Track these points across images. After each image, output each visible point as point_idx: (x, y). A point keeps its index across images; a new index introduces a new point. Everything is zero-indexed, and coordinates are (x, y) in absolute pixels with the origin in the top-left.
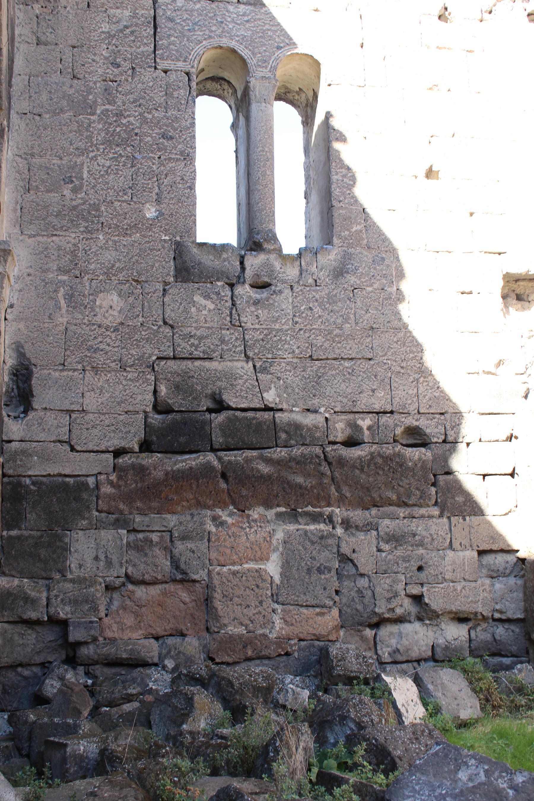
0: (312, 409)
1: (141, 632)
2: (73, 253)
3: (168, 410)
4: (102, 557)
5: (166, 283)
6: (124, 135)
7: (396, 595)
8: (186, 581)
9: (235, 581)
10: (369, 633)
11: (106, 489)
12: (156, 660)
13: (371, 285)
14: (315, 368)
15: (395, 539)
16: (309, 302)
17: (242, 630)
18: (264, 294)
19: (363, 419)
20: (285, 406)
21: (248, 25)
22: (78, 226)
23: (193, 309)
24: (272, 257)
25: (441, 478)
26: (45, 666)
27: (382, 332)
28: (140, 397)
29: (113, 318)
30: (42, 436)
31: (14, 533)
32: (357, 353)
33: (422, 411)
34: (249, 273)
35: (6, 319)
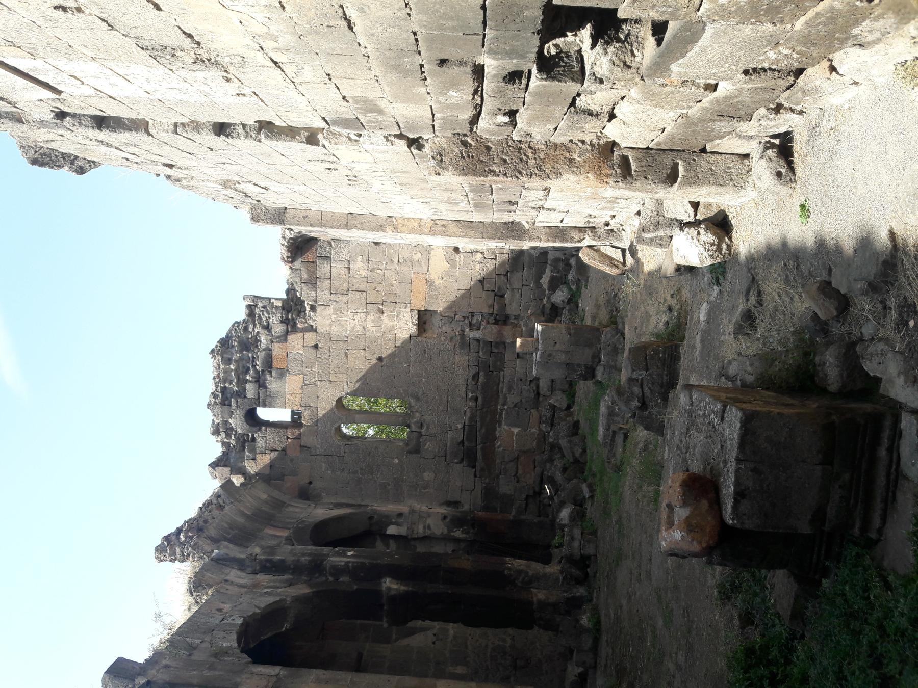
8: (518, 458)
10: (541, 399)
15: (510, 388)
17: (535, 443)
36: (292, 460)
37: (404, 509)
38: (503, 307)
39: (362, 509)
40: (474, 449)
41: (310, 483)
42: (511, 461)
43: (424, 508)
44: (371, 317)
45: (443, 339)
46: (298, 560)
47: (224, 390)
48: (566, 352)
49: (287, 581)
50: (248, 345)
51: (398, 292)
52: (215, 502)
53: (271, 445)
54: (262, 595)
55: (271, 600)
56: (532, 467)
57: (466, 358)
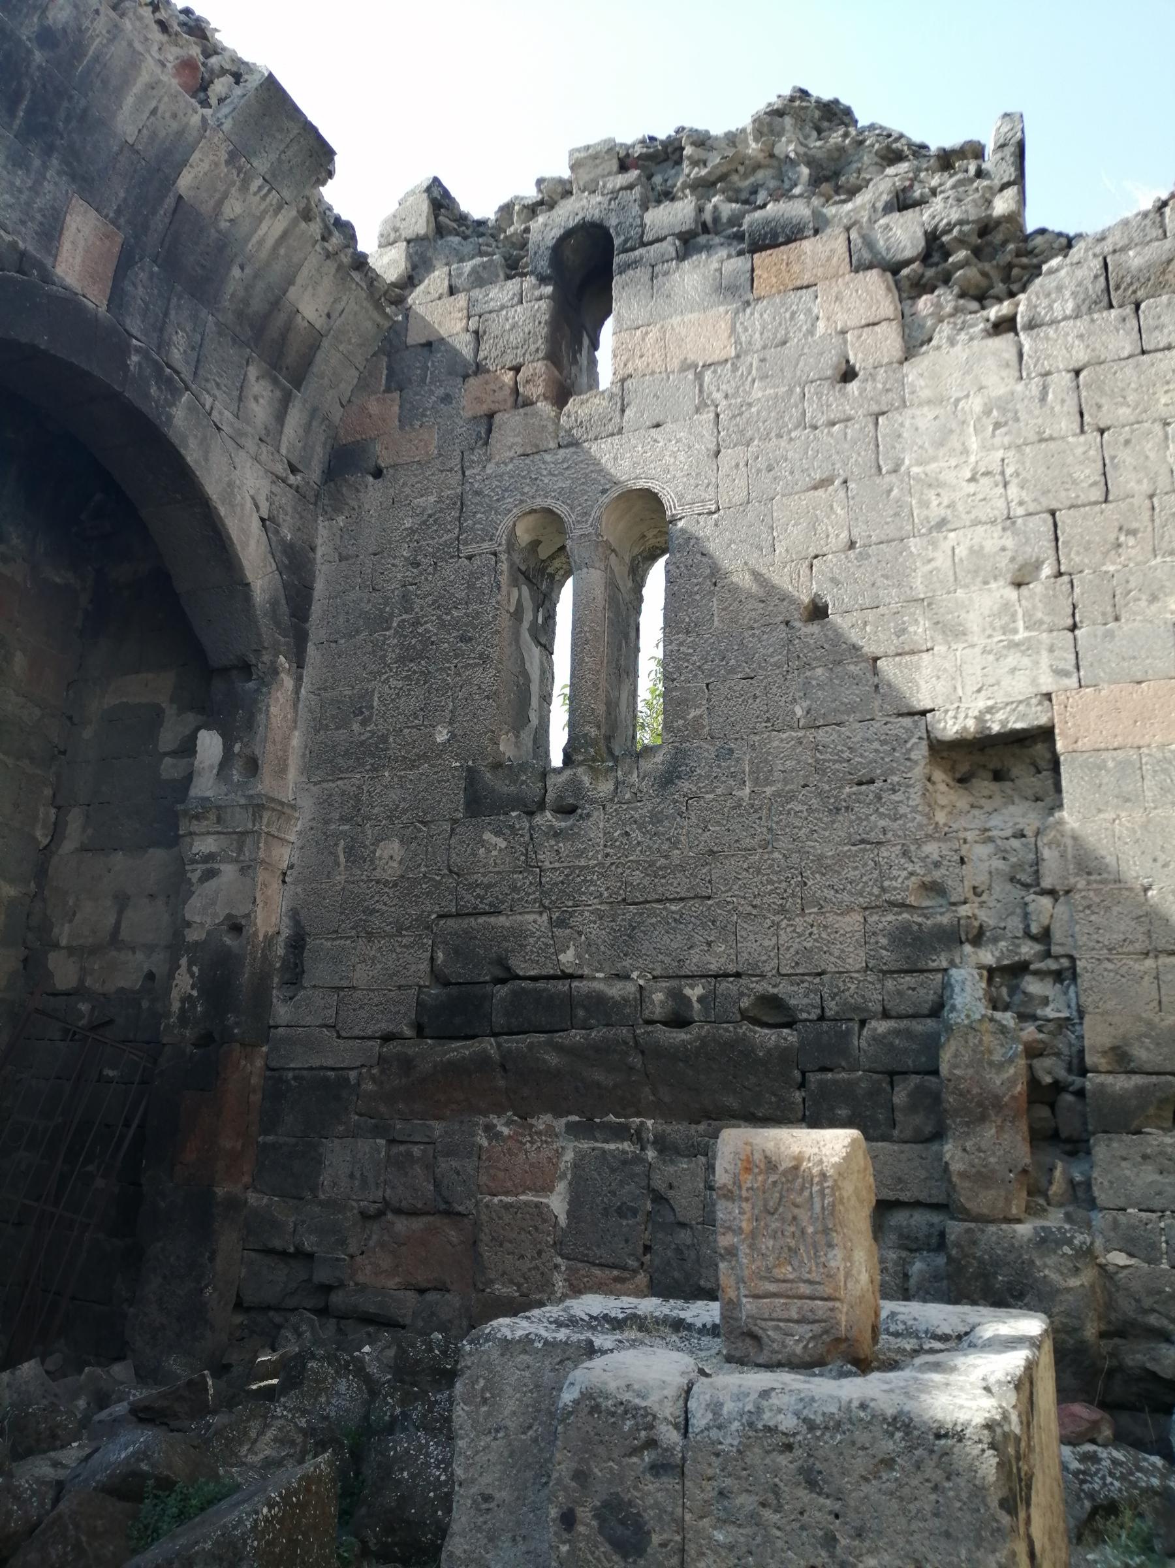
0: (621, 973)
1: (397, 1280)
3: (447, 984)
4: (358, 1175)
5: (455, 821)
6: (419, 647)
8: (449, 1213)
9: (507, 1218)
11: (368, 1086)
12: (408, 1321)
13: (713, 791)
14: (628, 917)
16: (625, 825)
19: (692, 987)
20: (586, 971)
21: (567, 473)
22: (363, 765)
23: (482, 850)
24: (580, 770)
25: (813, 1078)
27: (726, 857)
28: (413, 968)
29: (392, 870)
30: (309, 1020)
31: (270, 1138)
32: (688, 890)
33: (783, 971)
34: (550, 797)
35: (284, 882)
36: (447, 399)
38: (1124, 1119)
40: (491, 1028)
41: (378, 473)
44: (993, 540)
45: (932, 849)
50: (832, 177)
51: (1125, 627)
53: (495, 325)
57: (856, 960)
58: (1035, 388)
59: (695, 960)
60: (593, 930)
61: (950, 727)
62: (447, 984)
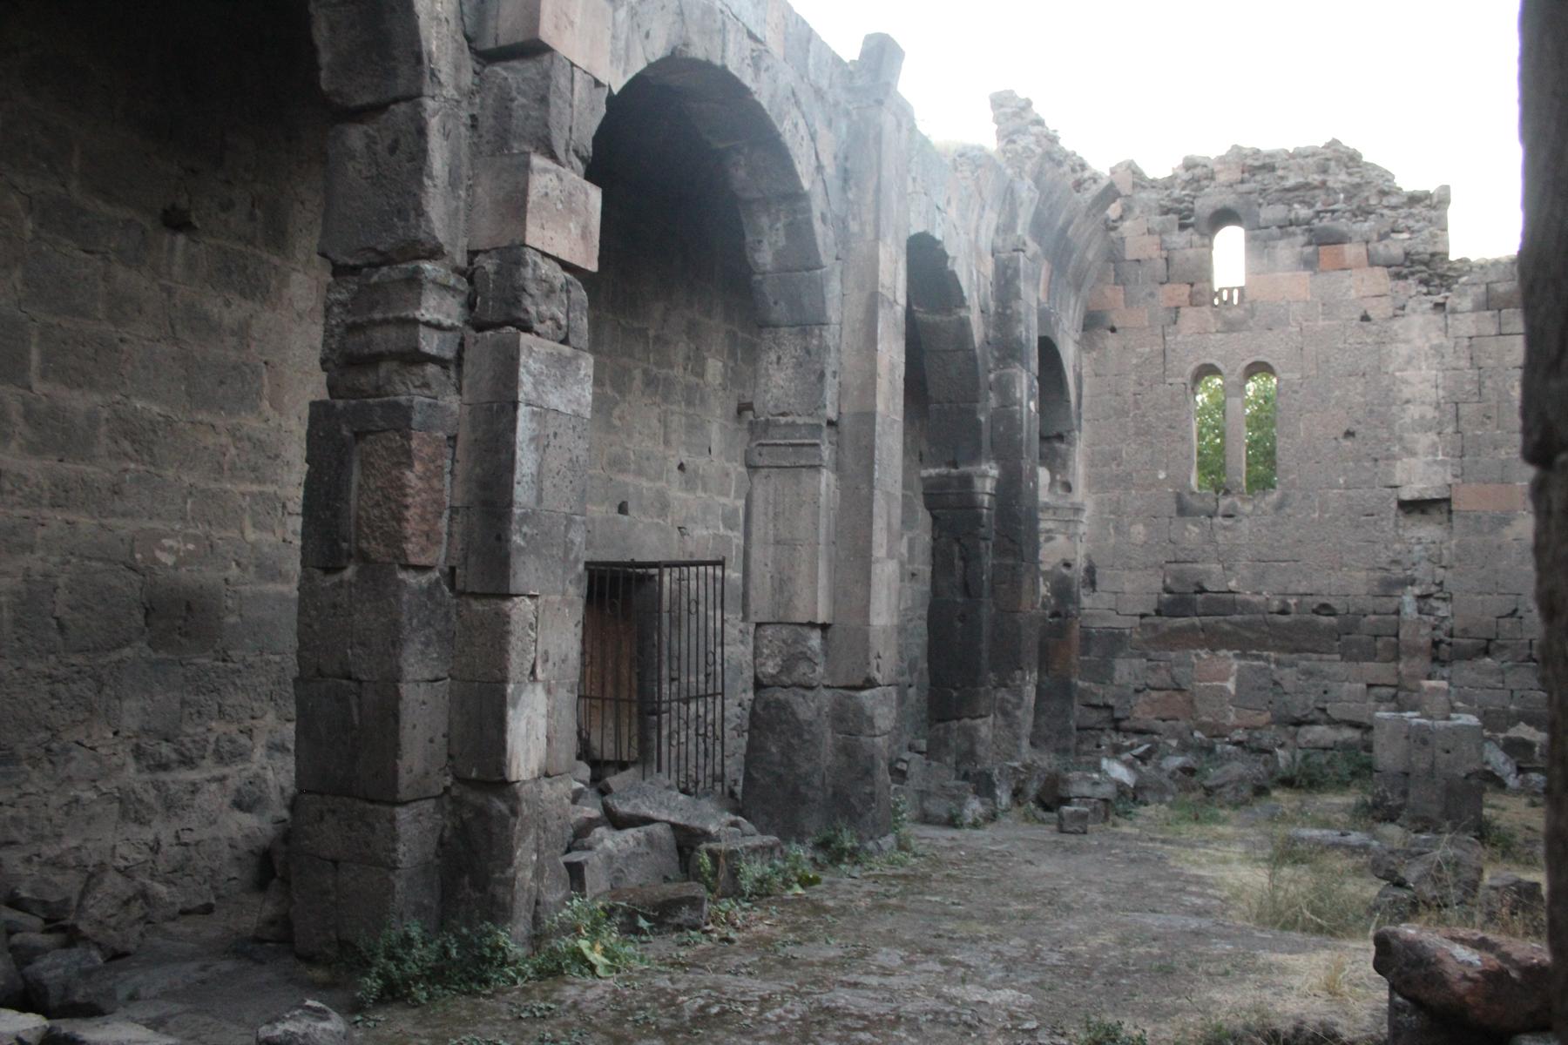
2: (1118, 502)
7: (1307, 707)
8: (1180, 690)
10: (1291, 728)
11: (1136, 636)
15: (1309, 673)
18: (1228, 522)
26: (1102, 730)
29: (1141, 538)
34: (1221, 510)
36: (1152, 295)
37: (1080, 494)
39: (1075, 422)
41: (1113, 330)
42: (1173, 679)
43: (1082, 529)
44: (1430, 413)
45: (1397, 546)
46: (1020, 321)
47: (1269, 168)
48: (1431, 772)
49: (987, 305)
52: (1087, 174)
53: (1177, 257)
54: (969, 265)
55: (964, 283)
56: (1164, 715)
57: (1363, 590)
58: (1452, 344)
59: (1292, 588)
60: (1245, 573)
61: (1406, 495)
62: (1171, 592)
